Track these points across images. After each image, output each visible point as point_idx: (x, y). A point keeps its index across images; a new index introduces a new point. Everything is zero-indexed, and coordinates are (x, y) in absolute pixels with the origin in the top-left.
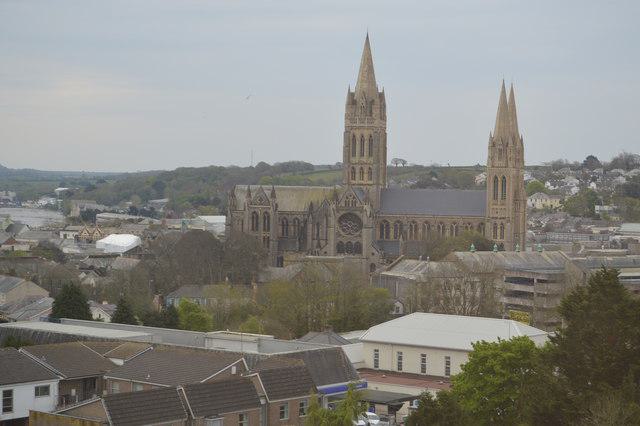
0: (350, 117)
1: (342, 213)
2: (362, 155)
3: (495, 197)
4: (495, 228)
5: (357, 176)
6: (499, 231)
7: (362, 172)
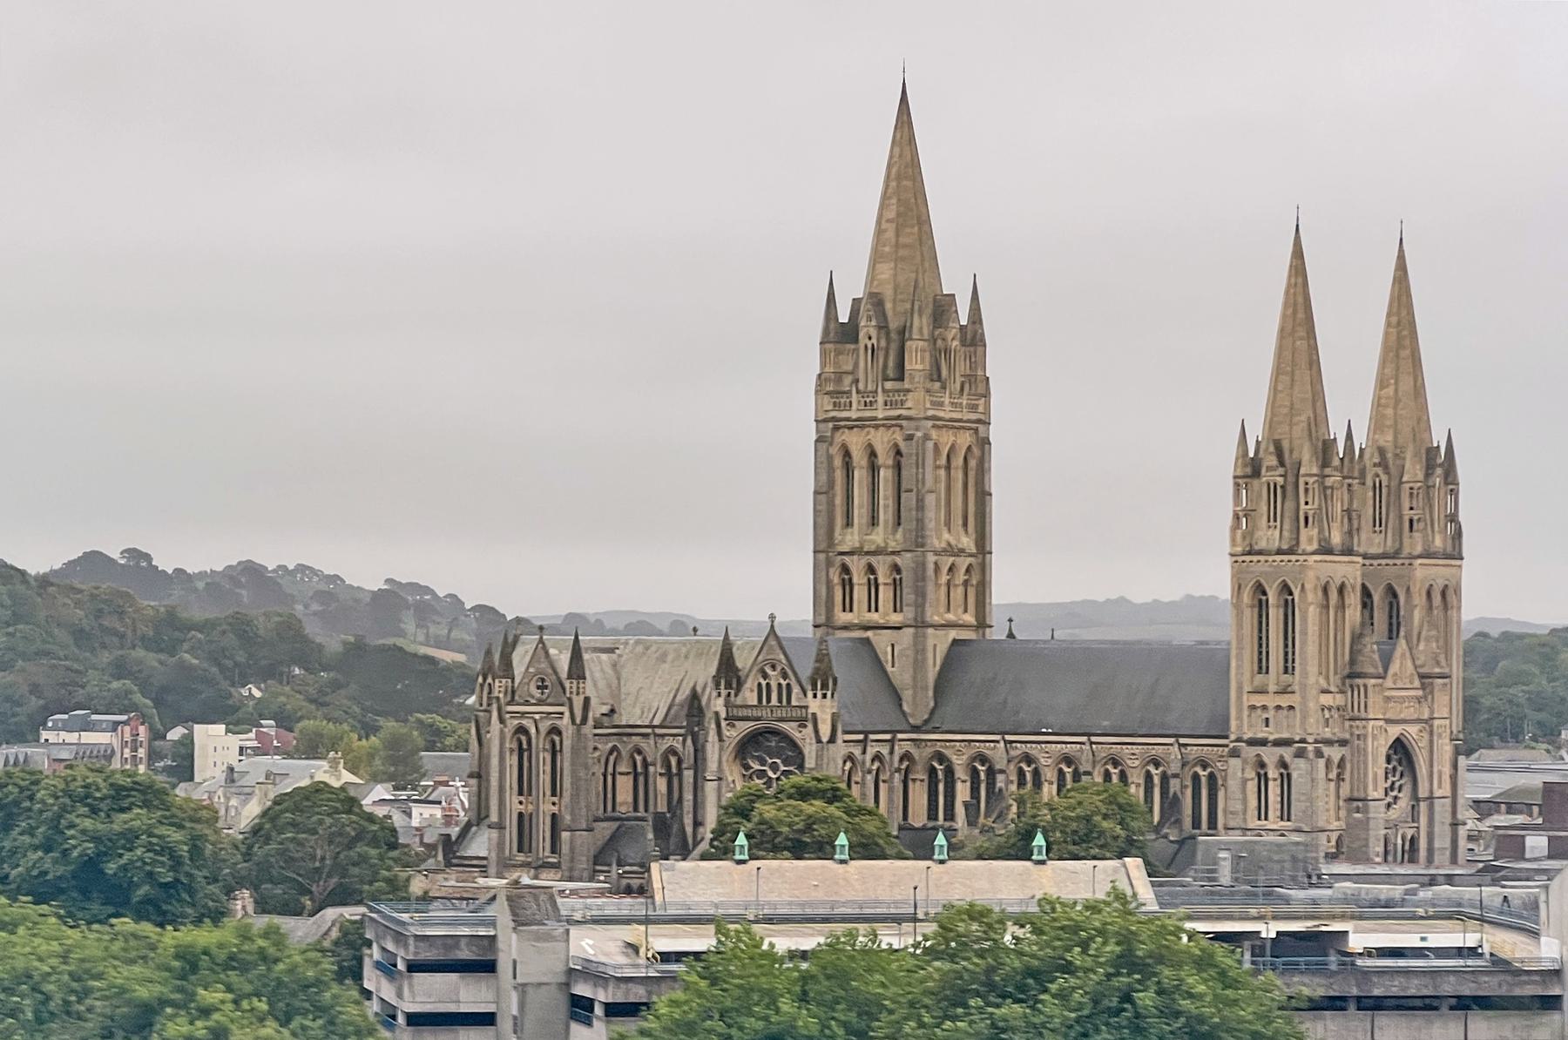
0: (831, 387)
1: (745, 727)
2: (874, 521)
3: (1262, 667)
4: (1262, 779)
5: (860, 593)
6: (1274, 789)
7: (873, 586)
